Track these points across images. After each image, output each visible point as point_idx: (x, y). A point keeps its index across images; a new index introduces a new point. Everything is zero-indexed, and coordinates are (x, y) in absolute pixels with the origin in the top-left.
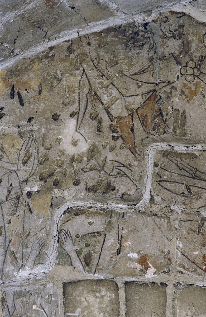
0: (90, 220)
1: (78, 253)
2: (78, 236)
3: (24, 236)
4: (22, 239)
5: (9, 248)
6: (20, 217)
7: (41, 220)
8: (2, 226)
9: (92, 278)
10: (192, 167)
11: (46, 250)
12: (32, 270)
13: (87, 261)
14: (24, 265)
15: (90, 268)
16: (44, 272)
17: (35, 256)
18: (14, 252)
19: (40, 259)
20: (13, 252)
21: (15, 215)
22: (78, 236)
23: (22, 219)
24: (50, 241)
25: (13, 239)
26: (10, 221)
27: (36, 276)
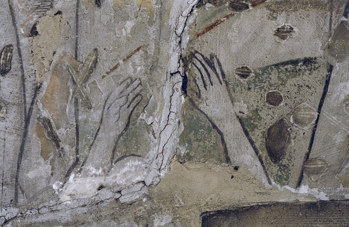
0: (281, 21)
1: (246, 124)
2: (244, 73)
3: (79, 71)
4: (74, 83)
5: (34, 111)
6: (64, 15)
7: (130, 24)
8: (11, 45)
9: (292, 200)
11: (148, 117)
12: (107, 175)
13: (274, 147)
14: (81, 160)
15: (285, 167)
16: (143, 182)
17: (114, 134)
18: (49, 122)
19: (129, 142)
20: (47, 123)
21: (48, 9)
22: (244, 73)
23: (72, 23)
24: (158, 89)
25: (45, 84)
26: (34, 27)
27: (119, 192)
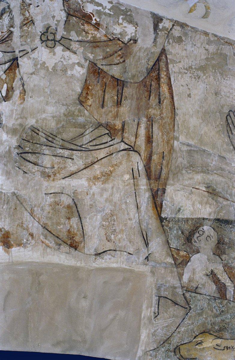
10: (55, 136)
